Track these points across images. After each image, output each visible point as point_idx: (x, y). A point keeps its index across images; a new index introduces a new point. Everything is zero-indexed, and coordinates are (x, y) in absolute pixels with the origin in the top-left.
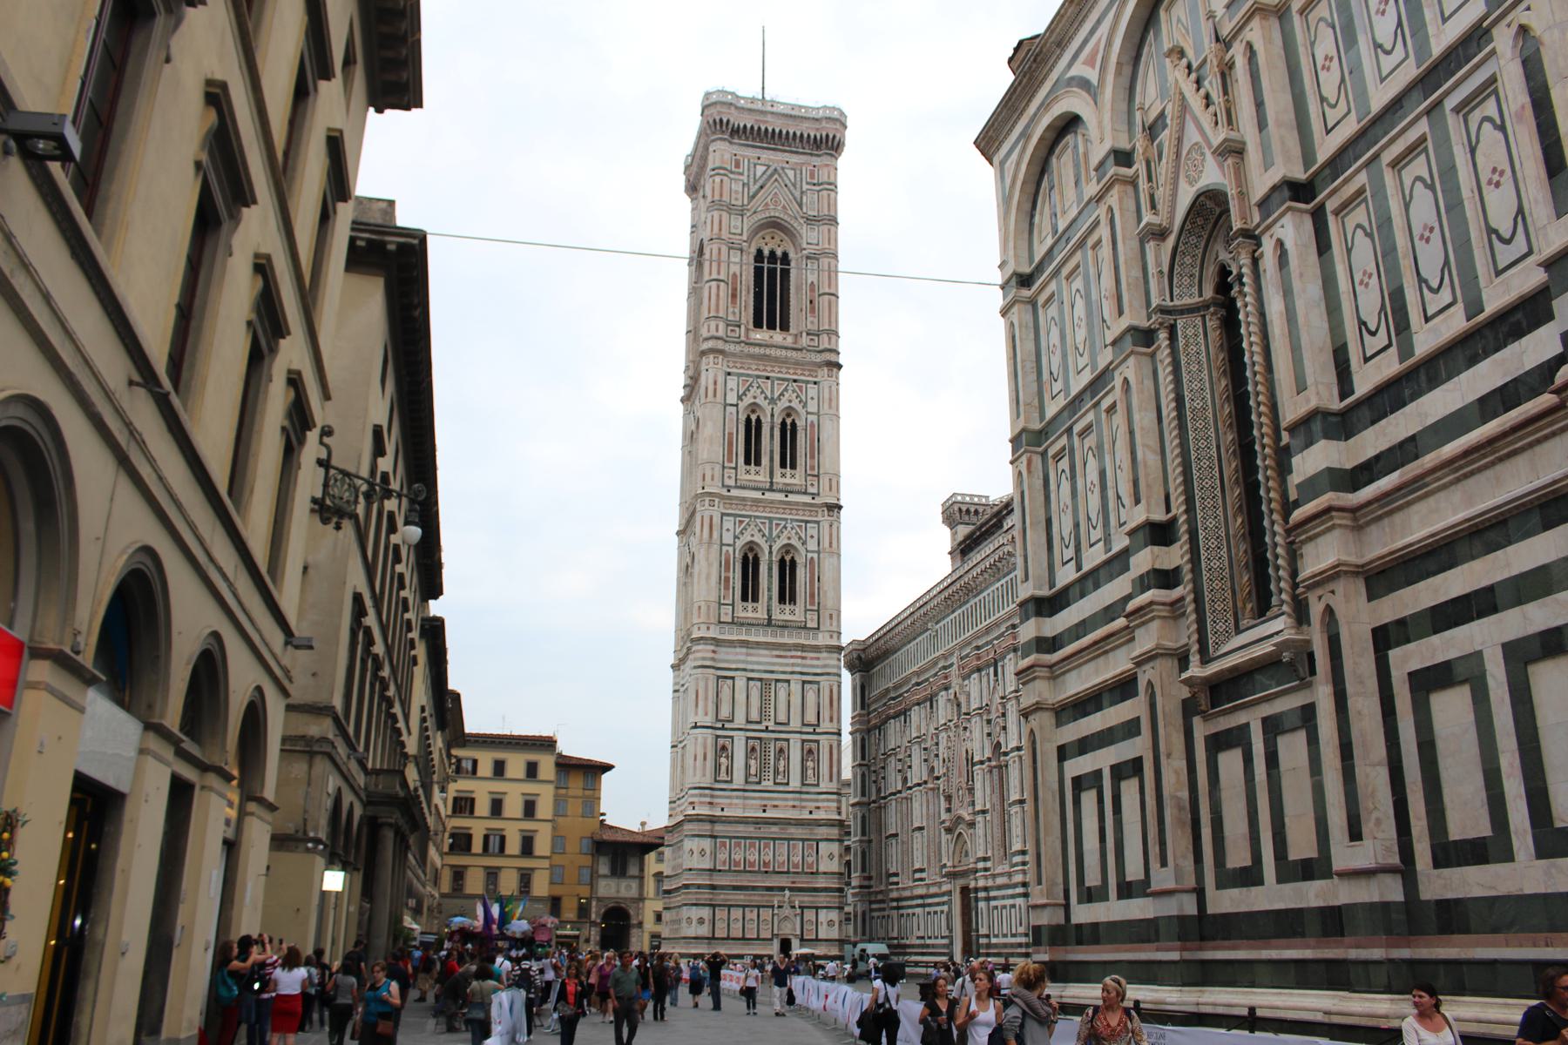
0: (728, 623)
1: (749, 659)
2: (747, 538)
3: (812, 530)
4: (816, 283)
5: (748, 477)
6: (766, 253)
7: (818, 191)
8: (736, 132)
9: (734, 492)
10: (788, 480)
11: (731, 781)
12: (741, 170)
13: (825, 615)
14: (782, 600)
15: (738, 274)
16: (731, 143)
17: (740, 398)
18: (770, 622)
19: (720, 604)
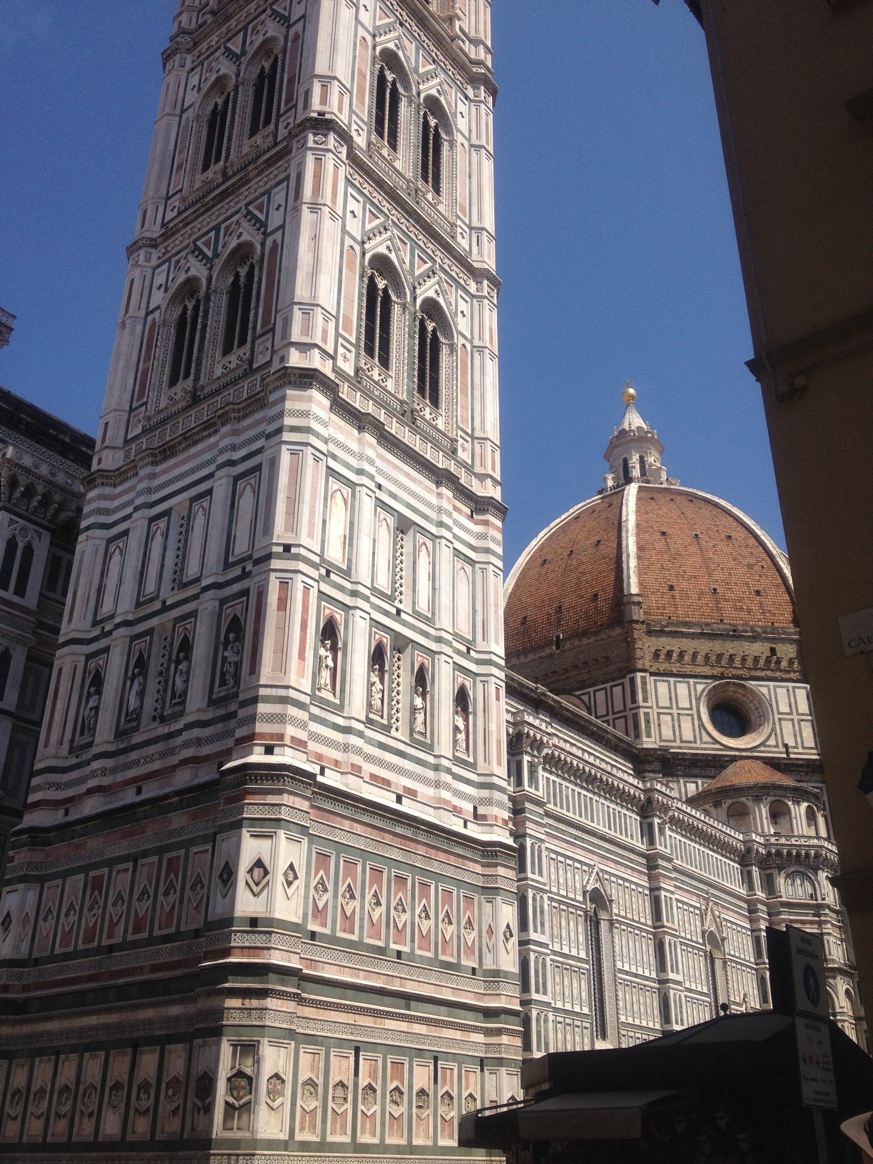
1: (157, 482)
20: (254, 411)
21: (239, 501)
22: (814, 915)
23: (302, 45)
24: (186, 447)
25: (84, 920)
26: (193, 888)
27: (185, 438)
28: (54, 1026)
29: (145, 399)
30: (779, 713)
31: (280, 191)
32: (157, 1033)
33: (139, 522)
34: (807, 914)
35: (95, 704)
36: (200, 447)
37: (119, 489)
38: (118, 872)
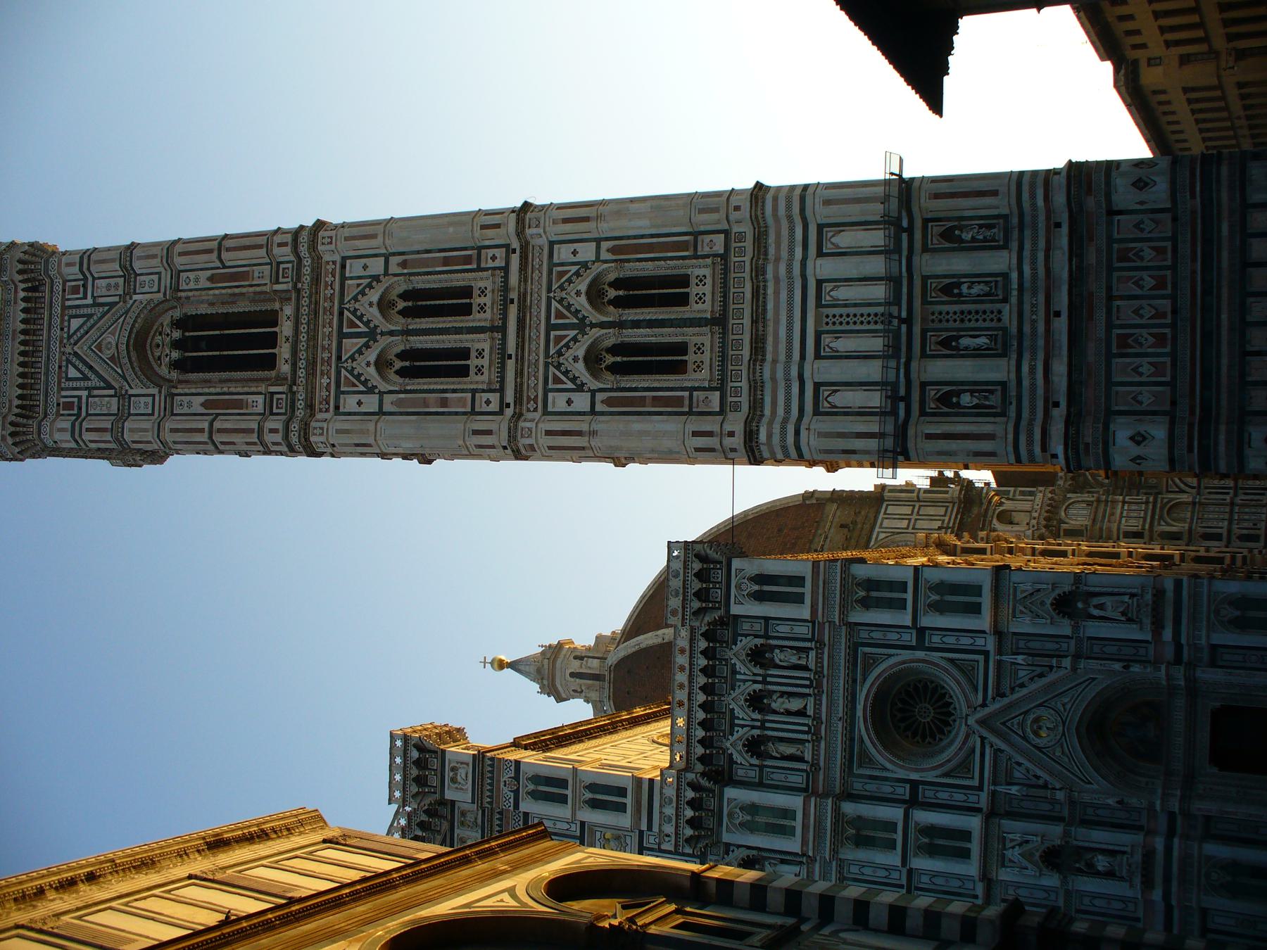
0: (722, 398)
1: (782, 357)
2: (580, 369)
3: (563, 253)
4: (209, 273)
5: (485, 371)
6: (175, 355)
7: (94, 279)
8: (27, 408)
9: (510, 398)
10: (487, 300)
11: (1004, 385)
12: (76, 400)
13: (706, 221)
14: (683, 300)
15: (202, 399)
16: (43, 419)
17: (371, 390)
18: (719, 321)
19: (690, 413)
20: (766, 243)
21: (841, 248)
22: (1106, 505)
23: (418, 252)
24: (764, 323)
25: (1150, 350)
26: (1142, 230)
27: (757, 322)
28: (1225, 361)
29: (686, 394)
30: (907, 528)
31: (559, 253)
32: (1238, 243)
33: (815, 366)
34: (1105, 511)
35: (969, 394)
36: (770, 306)
37: (767, 412)
38: (1118, 319)
